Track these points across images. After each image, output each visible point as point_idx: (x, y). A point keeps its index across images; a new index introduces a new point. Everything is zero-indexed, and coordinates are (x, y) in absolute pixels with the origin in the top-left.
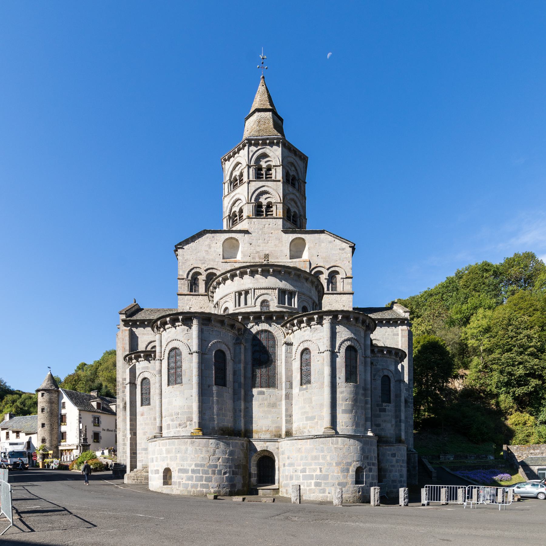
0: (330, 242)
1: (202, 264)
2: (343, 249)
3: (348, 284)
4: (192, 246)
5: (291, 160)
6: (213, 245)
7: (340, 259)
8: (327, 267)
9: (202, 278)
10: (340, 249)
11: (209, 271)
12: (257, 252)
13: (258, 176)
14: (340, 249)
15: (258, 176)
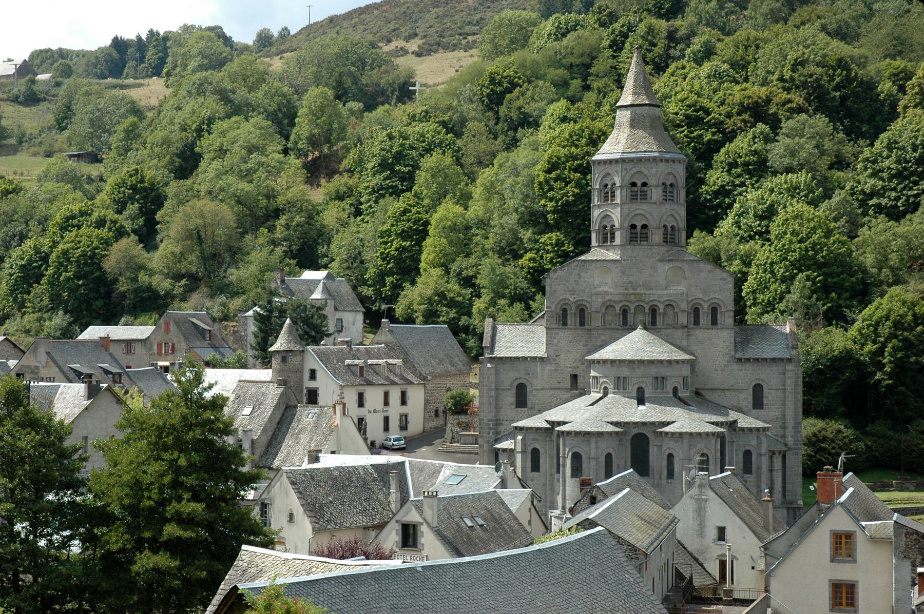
0: (710, 271)
1: (572, 294)
2: (724, 279)
3: (729, 317)
4: (560, 276)
5: (670, 170)
6: (583, 275)
7: (721, 290)
8: (707, 299)
9: (572, 310)
10: (720, 279)
11: (579, 303)
12: (631, 282)
13: (634, 197)
14: (720, 279)
15: (634, 197)
